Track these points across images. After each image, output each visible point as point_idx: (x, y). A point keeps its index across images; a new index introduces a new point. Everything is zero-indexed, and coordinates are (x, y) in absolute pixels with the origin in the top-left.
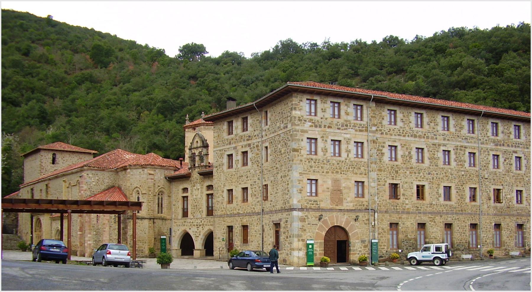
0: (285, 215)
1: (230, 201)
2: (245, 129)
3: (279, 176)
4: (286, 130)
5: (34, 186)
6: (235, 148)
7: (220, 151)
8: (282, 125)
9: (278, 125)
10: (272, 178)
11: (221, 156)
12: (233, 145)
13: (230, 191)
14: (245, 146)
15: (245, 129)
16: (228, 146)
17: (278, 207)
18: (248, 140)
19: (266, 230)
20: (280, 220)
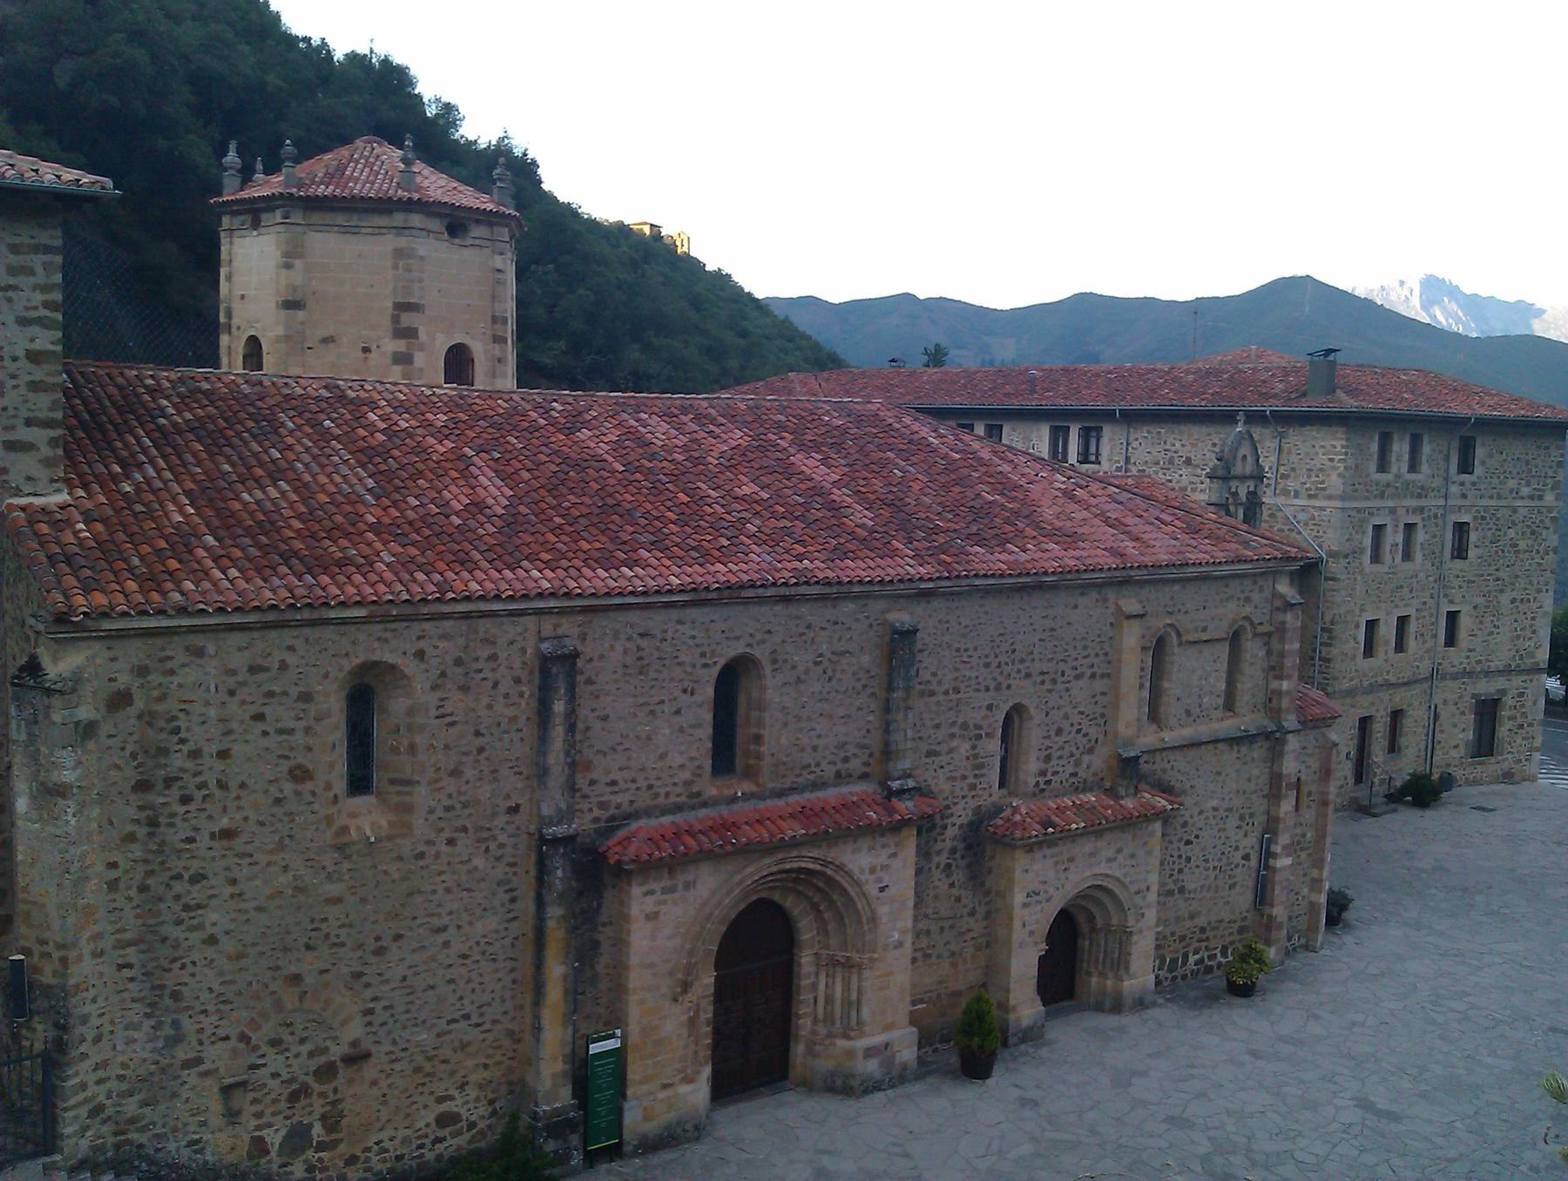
0: (1517, 681)
1: (1369, 651)
2: (1413, 467)
3: (1505, 599)
4: (1536, 503)
5: (568, 627)
6: (1393, 511)
7: (1358, 510)
8: (1525, 491)
9: (1512, 483)
10: (1480, 600)
11: (1360, 527)
12: (1391, 504)
13: (1372, 625)
14: (1415, 510)
15: (1413, 467)
16: (1378, 503)
17: (1497, 664)
18: (1420, 496)
19: (1443, 715)
20: (1504, 692)
